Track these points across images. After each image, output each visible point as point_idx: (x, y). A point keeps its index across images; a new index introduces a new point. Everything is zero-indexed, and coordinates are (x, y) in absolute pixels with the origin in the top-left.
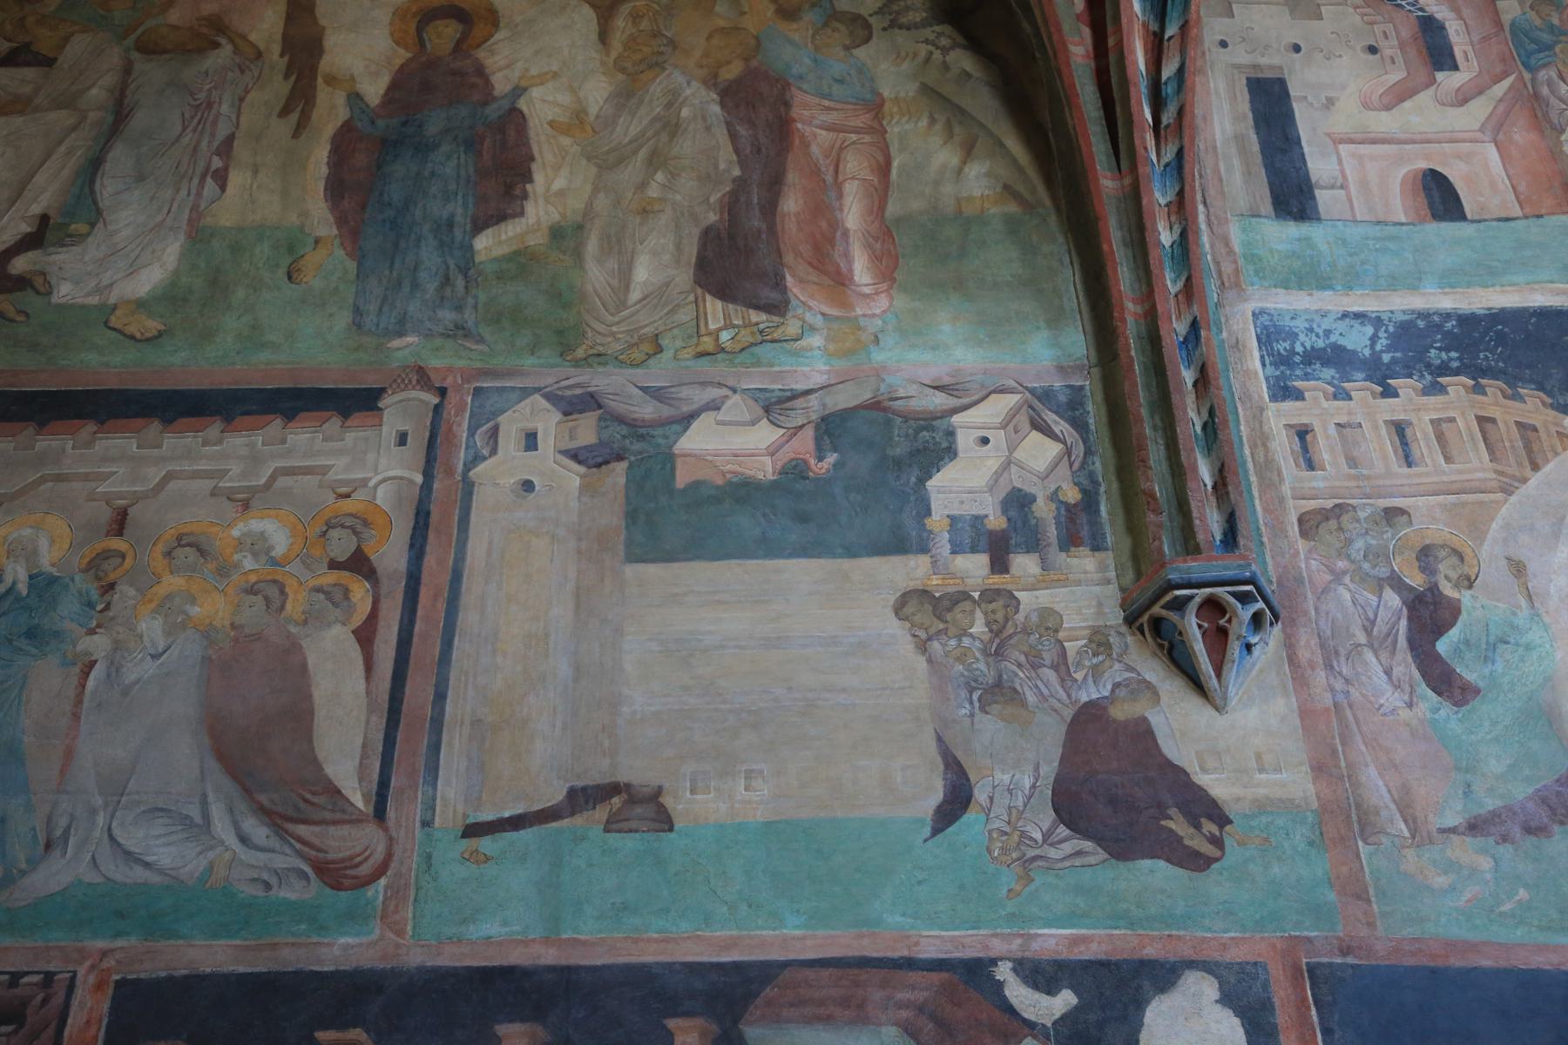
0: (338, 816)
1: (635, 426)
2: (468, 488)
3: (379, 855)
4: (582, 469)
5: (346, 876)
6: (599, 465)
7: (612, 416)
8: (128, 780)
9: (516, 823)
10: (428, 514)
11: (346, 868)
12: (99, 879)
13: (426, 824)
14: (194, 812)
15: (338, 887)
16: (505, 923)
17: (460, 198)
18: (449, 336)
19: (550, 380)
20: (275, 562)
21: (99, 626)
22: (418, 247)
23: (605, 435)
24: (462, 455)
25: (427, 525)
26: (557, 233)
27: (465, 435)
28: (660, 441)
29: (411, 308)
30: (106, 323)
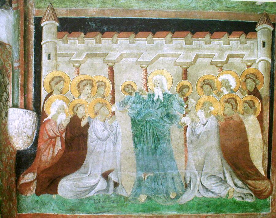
5: (261, 195)
8: (203, 166)
14: (222, 176)
15: (260, 198)
20: (232, 91)
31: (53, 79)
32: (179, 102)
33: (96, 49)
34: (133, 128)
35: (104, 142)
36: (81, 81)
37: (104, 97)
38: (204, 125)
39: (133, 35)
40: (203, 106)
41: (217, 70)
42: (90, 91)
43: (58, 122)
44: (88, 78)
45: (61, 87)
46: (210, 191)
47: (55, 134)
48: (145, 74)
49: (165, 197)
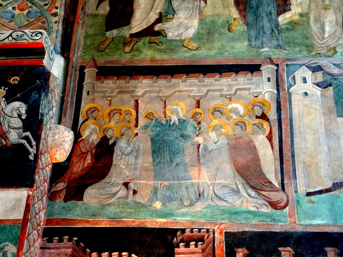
0: (272, 189)
1: (333, 76)
2: (290, 94)
3: (285, 198)
4: (320, 89)
5: (277, 206)
6: (325, 88)
7: (326, 73)
9: (320, 192)
10: (280, 102)
11: (277, 204)
12: (214, 205)
13: (296, 192)
14: (234, 187)
15: (276, 209)
16: (322, 220)
17: (272, 4)
18: (276, 48)
19: (307, 62)
21: (199, 134)
22: (263, 21)
23: (325, 78)
24: (286, 84)
25: (280, 106)
26: (301, 15)
27: (286, 78)
28: (341, 80)
29: (264, 39)
30: (183, 45)
31: (89, 109)
32: (192, 125)
33: (126, 88)
34: (152, 146)
35: (128, 157)
36: (112, 111)
37: (130, 122)
38: (215, 143)
39: (155, 77)
40: (215, 128)
41: (227, 101)
42: (118, 118)
43: (90, 141)
44: (118, 108)
45: (95, 115)
46: (223, 200)
47: (87, 150)
48: (164, 105)
49: (179, 204)
